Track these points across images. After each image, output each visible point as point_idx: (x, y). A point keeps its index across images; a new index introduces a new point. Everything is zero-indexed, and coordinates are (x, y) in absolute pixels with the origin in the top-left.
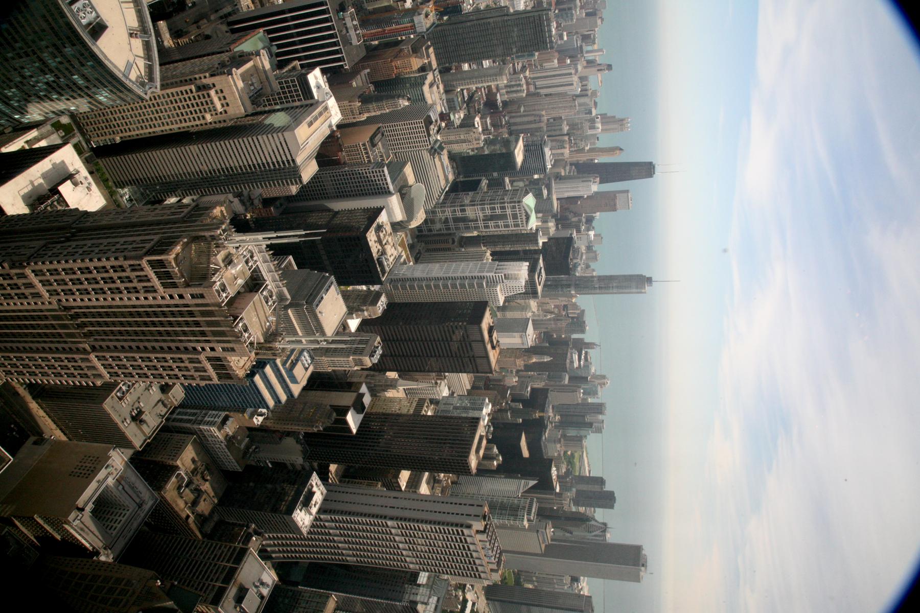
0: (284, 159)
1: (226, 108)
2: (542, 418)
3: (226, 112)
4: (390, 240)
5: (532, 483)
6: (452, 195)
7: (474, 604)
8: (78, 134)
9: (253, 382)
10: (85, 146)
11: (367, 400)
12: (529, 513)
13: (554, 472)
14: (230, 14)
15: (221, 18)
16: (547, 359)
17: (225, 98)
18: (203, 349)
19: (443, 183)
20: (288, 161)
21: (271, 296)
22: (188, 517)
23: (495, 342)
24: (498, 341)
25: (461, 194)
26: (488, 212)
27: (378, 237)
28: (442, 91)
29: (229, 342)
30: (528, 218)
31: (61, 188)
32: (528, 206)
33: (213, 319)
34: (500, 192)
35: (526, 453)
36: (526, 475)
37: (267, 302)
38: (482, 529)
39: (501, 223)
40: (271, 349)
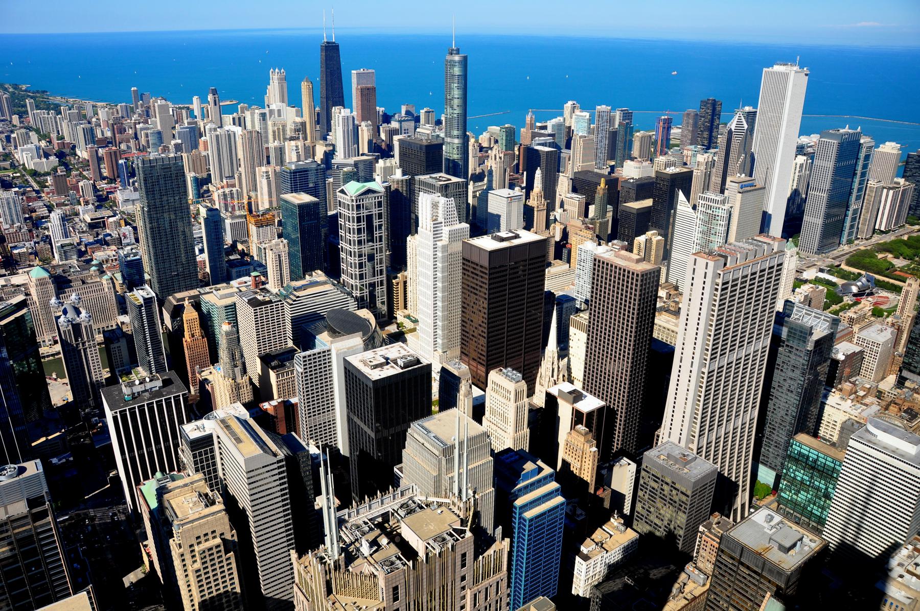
0: (276, 471)
1: (217, 534)
2: (607, 183)
3: (222, 534)
4: (382, 353)
5: (681, 196)
6: (344, 277)
7: (821, 270)
9: (531, 520)
11: (567, 387)
12: (716, 202)
13: (671, 170)
16: (538, 174)
17: (206, 535)
19: (328, 287)
20: (279, 468)
22: (685, 598)
23: (511, 235)
24: (510, 231)
25: (343, 266)
26: (364, 236)
27: (376, 367)
28: (225, 285)
30: (369, 191)
32: (358, 190)
34: (341, 221)
35: (648, 203)
36: (671, 203)
38: (723, 260)
39: (376, 222)
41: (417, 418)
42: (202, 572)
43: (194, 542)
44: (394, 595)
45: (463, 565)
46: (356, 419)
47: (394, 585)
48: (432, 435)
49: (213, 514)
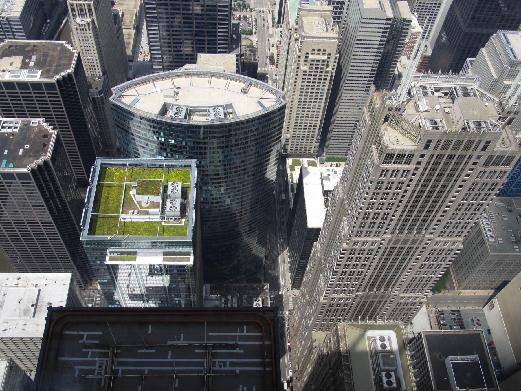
0: (383, 26)
1: (327, 53)
3: (329, 54)
8: (304, 159)
10: (313, 159)
14: (273, 19)
15: (273, 26)
17: (319, 50)
18: (475, 164)
20: (386, 24)
21: (467, 89)
29: (479, 142)
31: (325, 189)
33: (453, 143)
37: (470, 96)
40: (509, 113)
41: (504, 28)
42: (308, 73)
43: (310, 52)
44: (426, 145)
45: (484, 149)
46: (457, 11)
47: (430, 139)
48: (510, 47)
49: (330, 38)
